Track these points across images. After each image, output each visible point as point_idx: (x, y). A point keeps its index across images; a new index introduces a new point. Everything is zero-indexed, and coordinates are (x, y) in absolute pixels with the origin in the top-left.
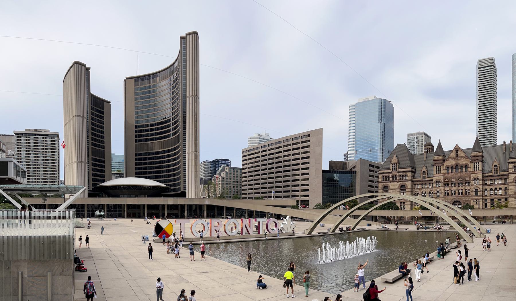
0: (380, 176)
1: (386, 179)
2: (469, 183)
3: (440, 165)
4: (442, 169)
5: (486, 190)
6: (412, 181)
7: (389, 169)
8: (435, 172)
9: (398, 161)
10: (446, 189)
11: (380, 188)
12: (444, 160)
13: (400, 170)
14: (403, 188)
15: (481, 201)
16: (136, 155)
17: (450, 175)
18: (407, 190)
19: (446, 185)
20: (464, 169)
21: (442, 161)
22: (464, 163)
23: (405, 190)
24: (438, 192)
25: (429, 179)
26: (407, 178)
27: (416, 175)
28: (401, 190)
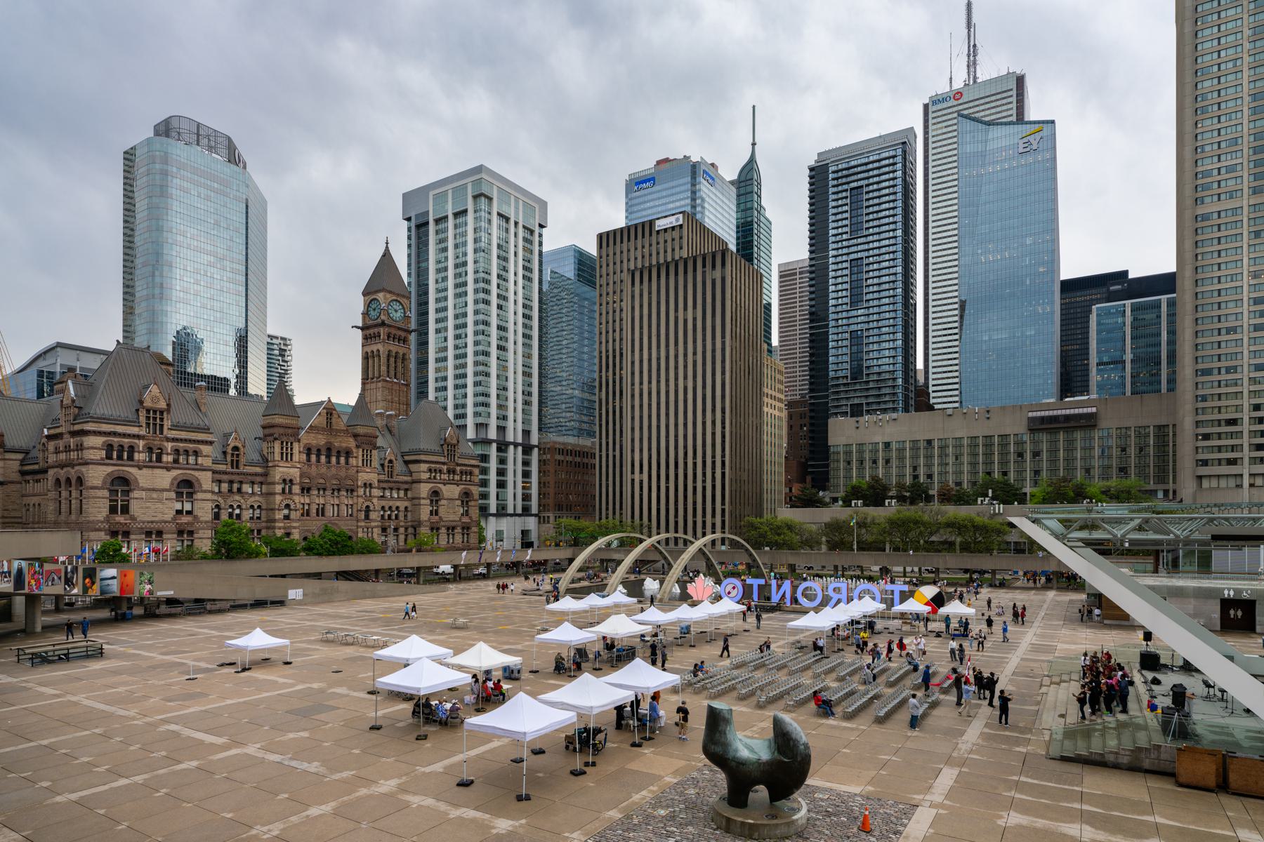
2: (352, 491)
3: (292, 439)
4: (296, 450)
6: (214, 472)
8: (277, 457)
18: (199, 496)
20: (342, 460)
23: (190, 495)
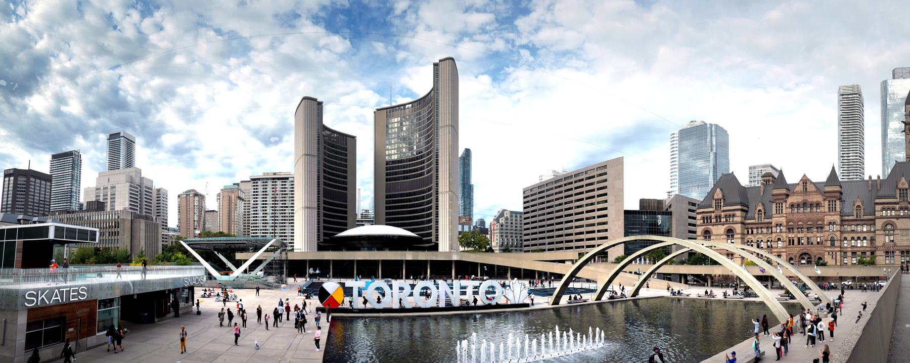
0: (699, 217)
1: (707, 220)
5: (845, 239)
6: (742, 223)
7: (711, 206)
8: (774, 212)
9: (723, 196)
10: (790, 235)
11: (699, 233)
12: (788, 196)
13: (725, 208)
14: (730, 233)
15: (838, 253)
16: (387, 197)
17: (795, 216)
18: (735, 236)
19: (790, 229)
21: (784, 197)
22: (815, 200)
23: (733, 236)
24: (779, 239)
25: (766, 221)
26: (735, 219)
27: (749, 214)
28: (728, 236)
